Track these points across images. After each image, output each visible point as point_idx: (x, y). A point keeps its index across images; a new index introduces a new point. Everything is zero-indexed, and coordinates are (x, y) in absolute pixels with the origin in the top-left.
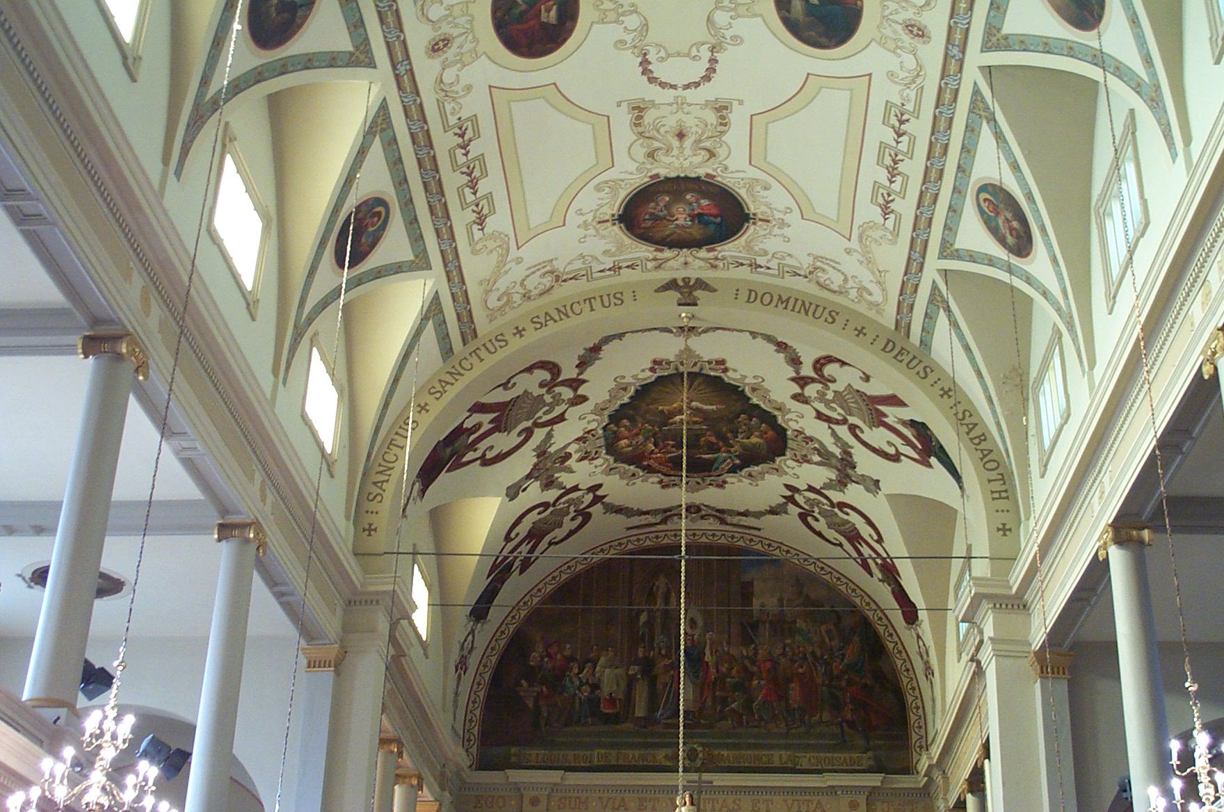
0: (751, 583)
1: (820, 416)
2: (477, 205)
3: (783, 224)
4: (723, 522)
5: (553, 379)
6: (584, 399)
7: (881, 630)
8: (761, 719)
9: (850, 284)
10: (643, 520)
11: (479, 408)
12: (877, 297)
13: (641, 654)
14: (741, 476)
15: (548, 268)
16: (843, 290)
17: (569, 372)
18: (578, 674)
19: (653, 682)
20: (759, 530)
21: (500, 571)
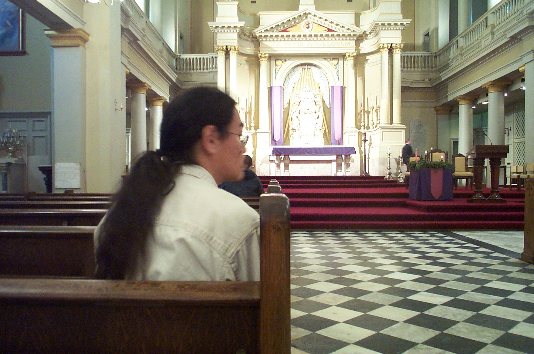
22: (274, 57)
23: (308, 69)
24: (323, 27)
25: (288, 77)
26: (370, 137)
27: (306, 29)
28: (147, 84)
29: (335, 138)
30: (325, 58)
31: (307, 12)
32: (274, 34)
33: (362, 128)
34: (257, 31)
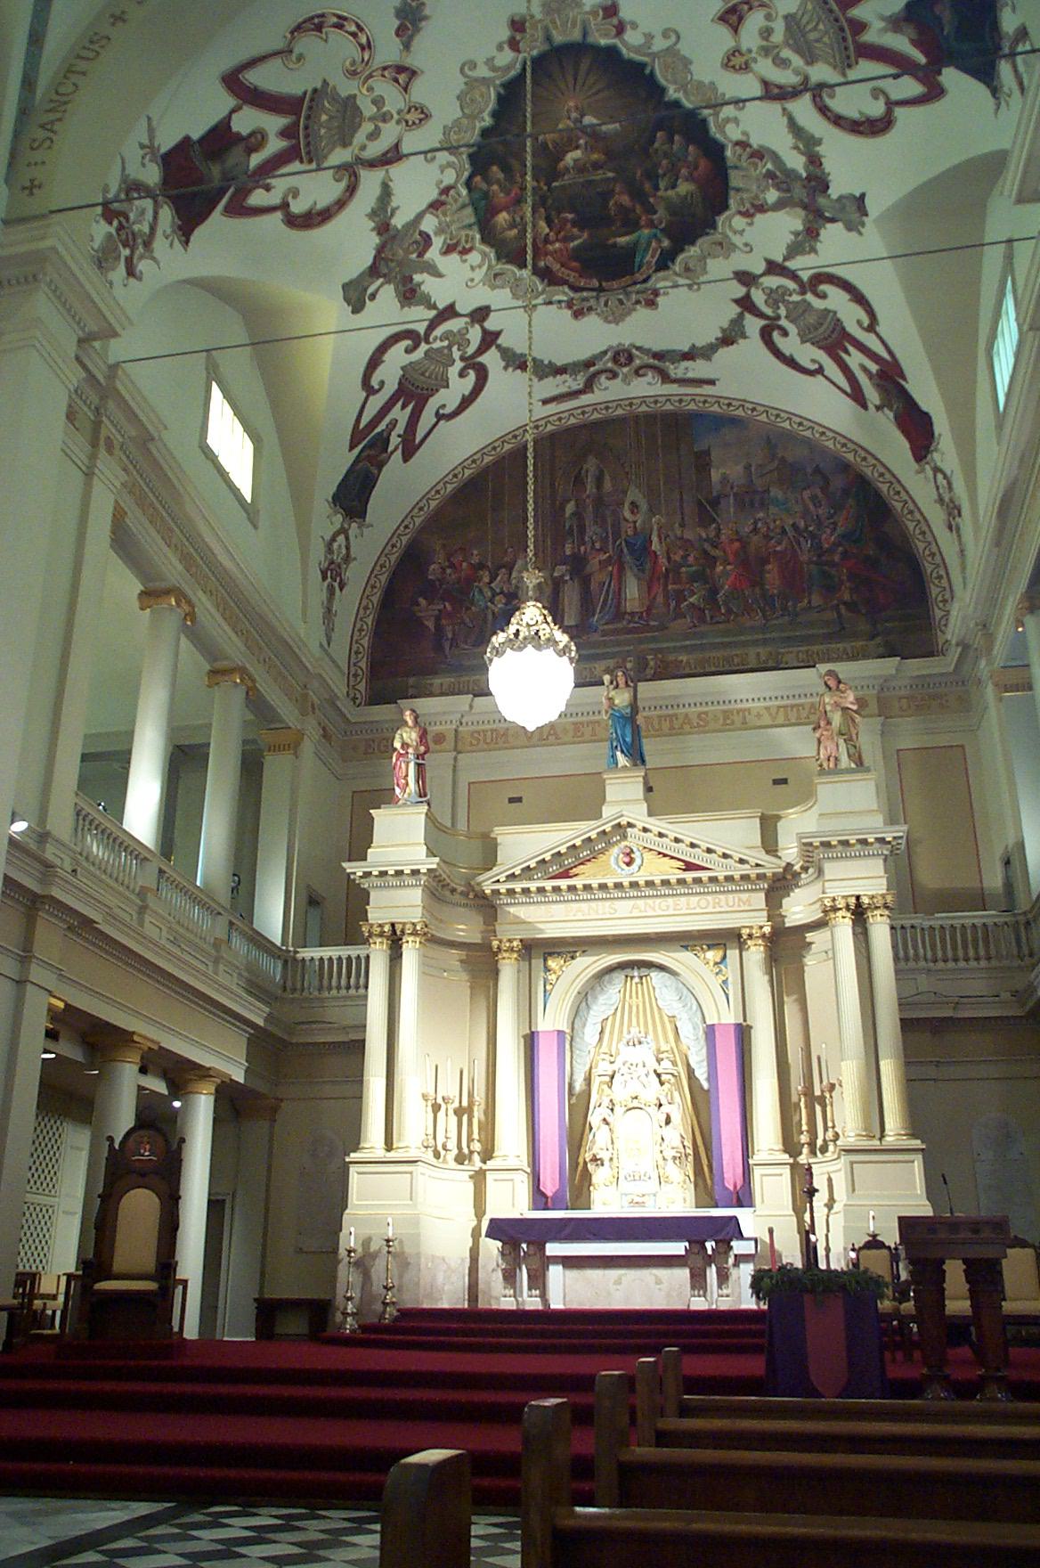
0: (707, 453)
4: (666, 378)
8: (729, 611)
14: (676, 274)
18: (491, 582)
19: (585, 582)
20: (712, 382)
22: (539, 950)
23: (641, 978)
24: (672, 858)
25: (584, 1004)
26: (830, 1180)
27: (624, 866)
28: (140, 1035)
29: (727, 1185)
30: (686, 943)
31: (624, 821)
32: (533, 886)
33: (805, 1150)
34: (484, 881)
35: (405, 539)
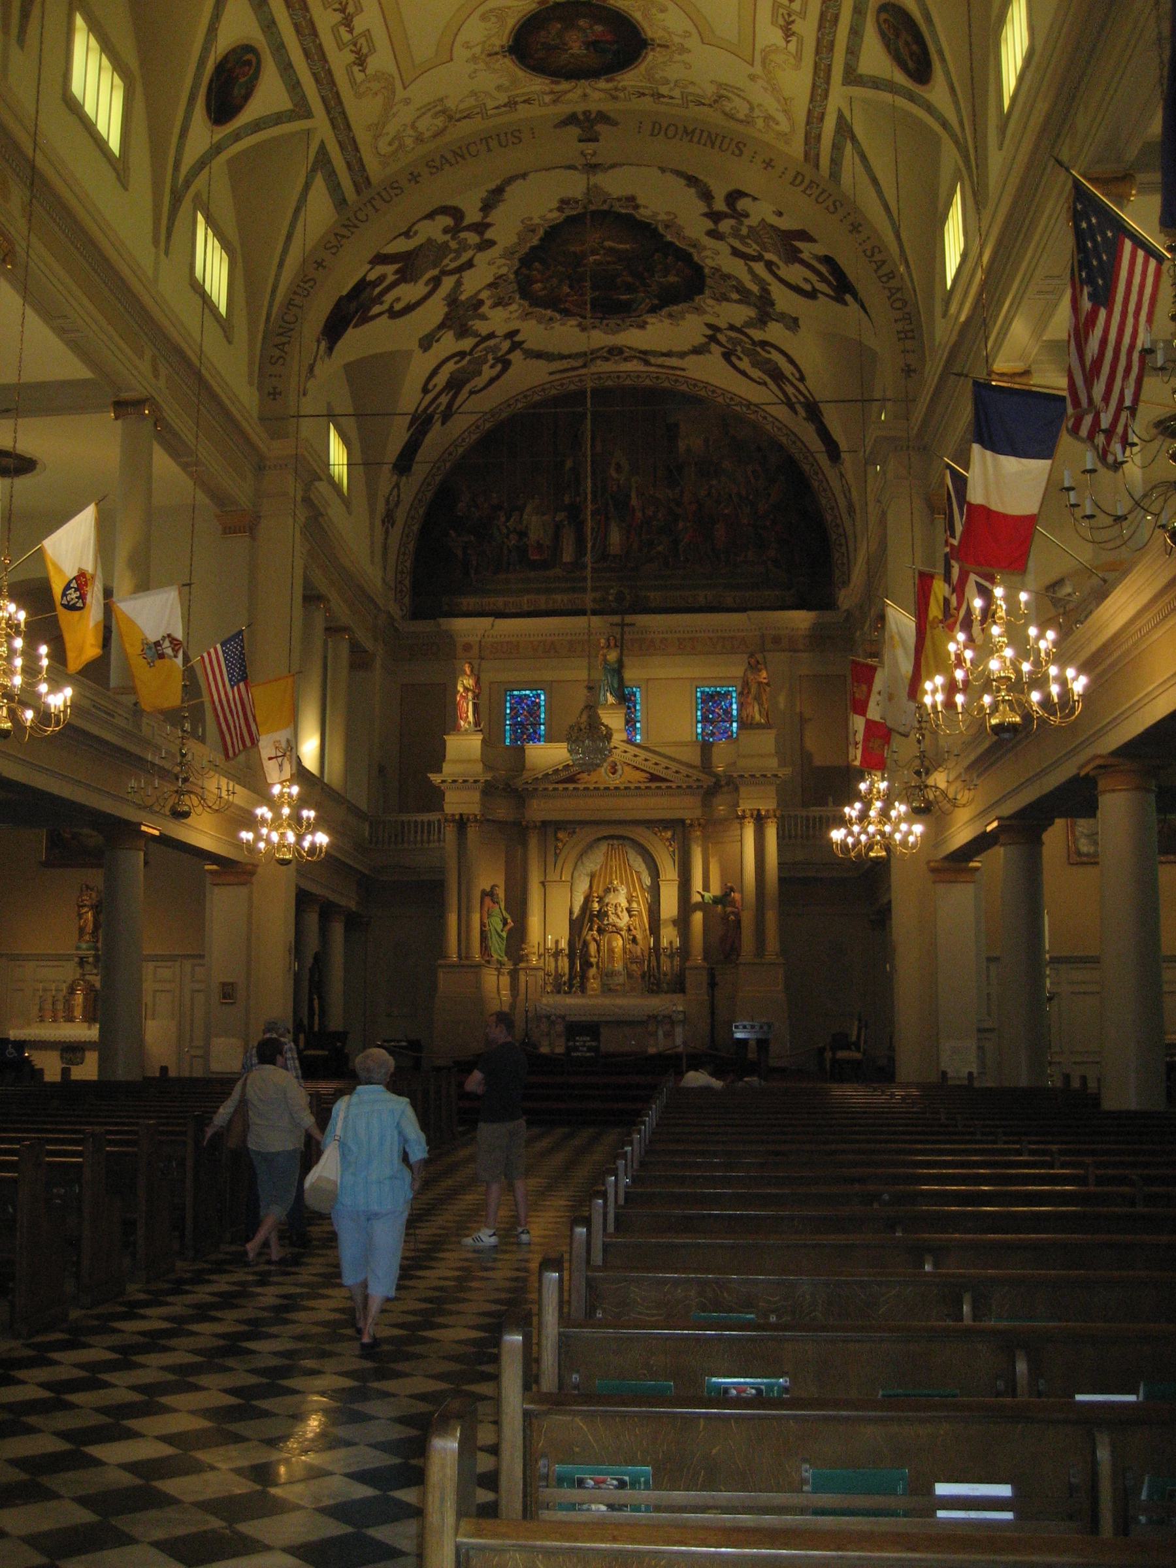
0: (677, 425)
1: (736, 253)
2: (355, 45)
3: (683, 50)
4: (647, 363)
5: (456, 224)
6: (491, 243)
7: (806, 467)
9: (757, 113)
10: (565, 364)
11: (380, 259)
12: (784, 127)
13: (567, 500)
15: (439, 108)
16: (750, 119)
17: (473, 215)
20: (683, 370)
21: (421, 423)
24: (642, 770)
32: (551, 787)
35: (438, 478)
